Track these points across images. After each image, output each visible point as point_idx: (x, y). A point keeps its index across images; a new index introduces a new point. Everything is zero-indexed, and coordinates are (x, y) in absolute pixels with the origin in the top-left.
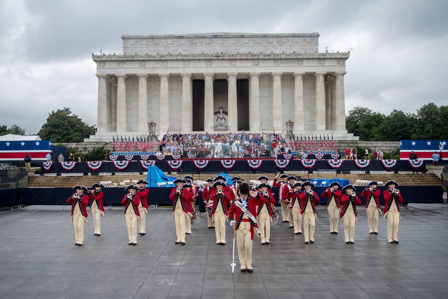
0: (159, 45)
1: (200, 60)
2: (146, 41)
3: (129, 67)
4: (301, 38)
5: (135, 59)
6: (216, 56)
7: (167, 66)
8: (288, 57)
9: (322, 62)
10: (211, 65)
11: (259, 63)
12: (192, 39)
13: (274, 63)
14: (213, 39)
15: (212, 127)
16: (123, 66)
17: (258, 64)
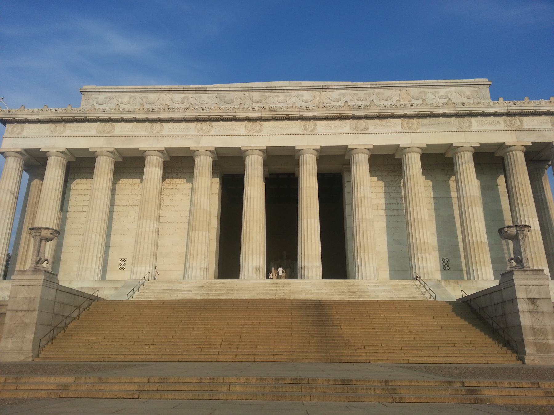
0: (156, 104)
1: (235, 120)
2: (130, 98)
3: (76, 134)
4: (453, 89)
5: (89, 117)
6: (271, 111)
7: (163, 133)
8: (436, 111)
9: (516, 120)
10: (261, 130)
11: (367, 125)
12: (222, 94)
13: (403, 125)
14: (267, 94)
15: (257, 269)
16: (63, 132)
17: (367, 128)
